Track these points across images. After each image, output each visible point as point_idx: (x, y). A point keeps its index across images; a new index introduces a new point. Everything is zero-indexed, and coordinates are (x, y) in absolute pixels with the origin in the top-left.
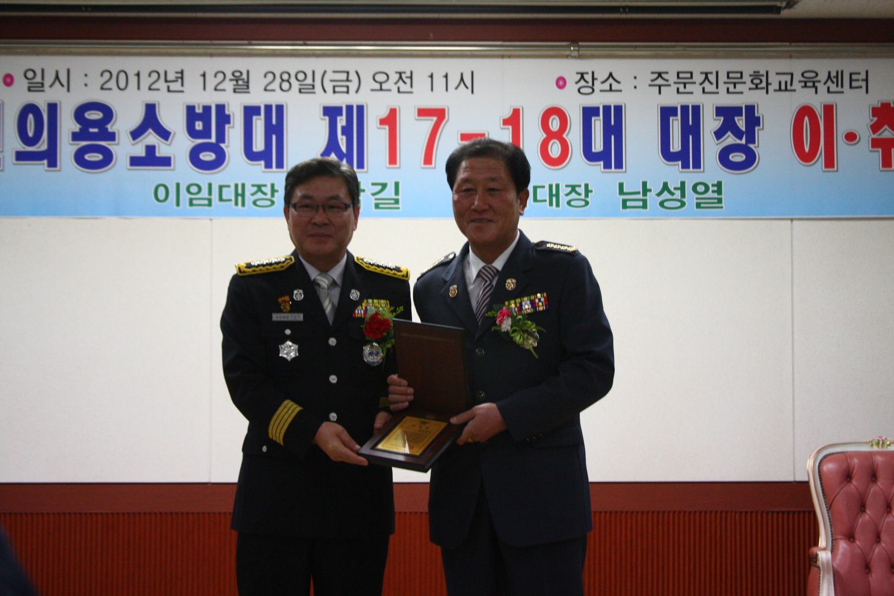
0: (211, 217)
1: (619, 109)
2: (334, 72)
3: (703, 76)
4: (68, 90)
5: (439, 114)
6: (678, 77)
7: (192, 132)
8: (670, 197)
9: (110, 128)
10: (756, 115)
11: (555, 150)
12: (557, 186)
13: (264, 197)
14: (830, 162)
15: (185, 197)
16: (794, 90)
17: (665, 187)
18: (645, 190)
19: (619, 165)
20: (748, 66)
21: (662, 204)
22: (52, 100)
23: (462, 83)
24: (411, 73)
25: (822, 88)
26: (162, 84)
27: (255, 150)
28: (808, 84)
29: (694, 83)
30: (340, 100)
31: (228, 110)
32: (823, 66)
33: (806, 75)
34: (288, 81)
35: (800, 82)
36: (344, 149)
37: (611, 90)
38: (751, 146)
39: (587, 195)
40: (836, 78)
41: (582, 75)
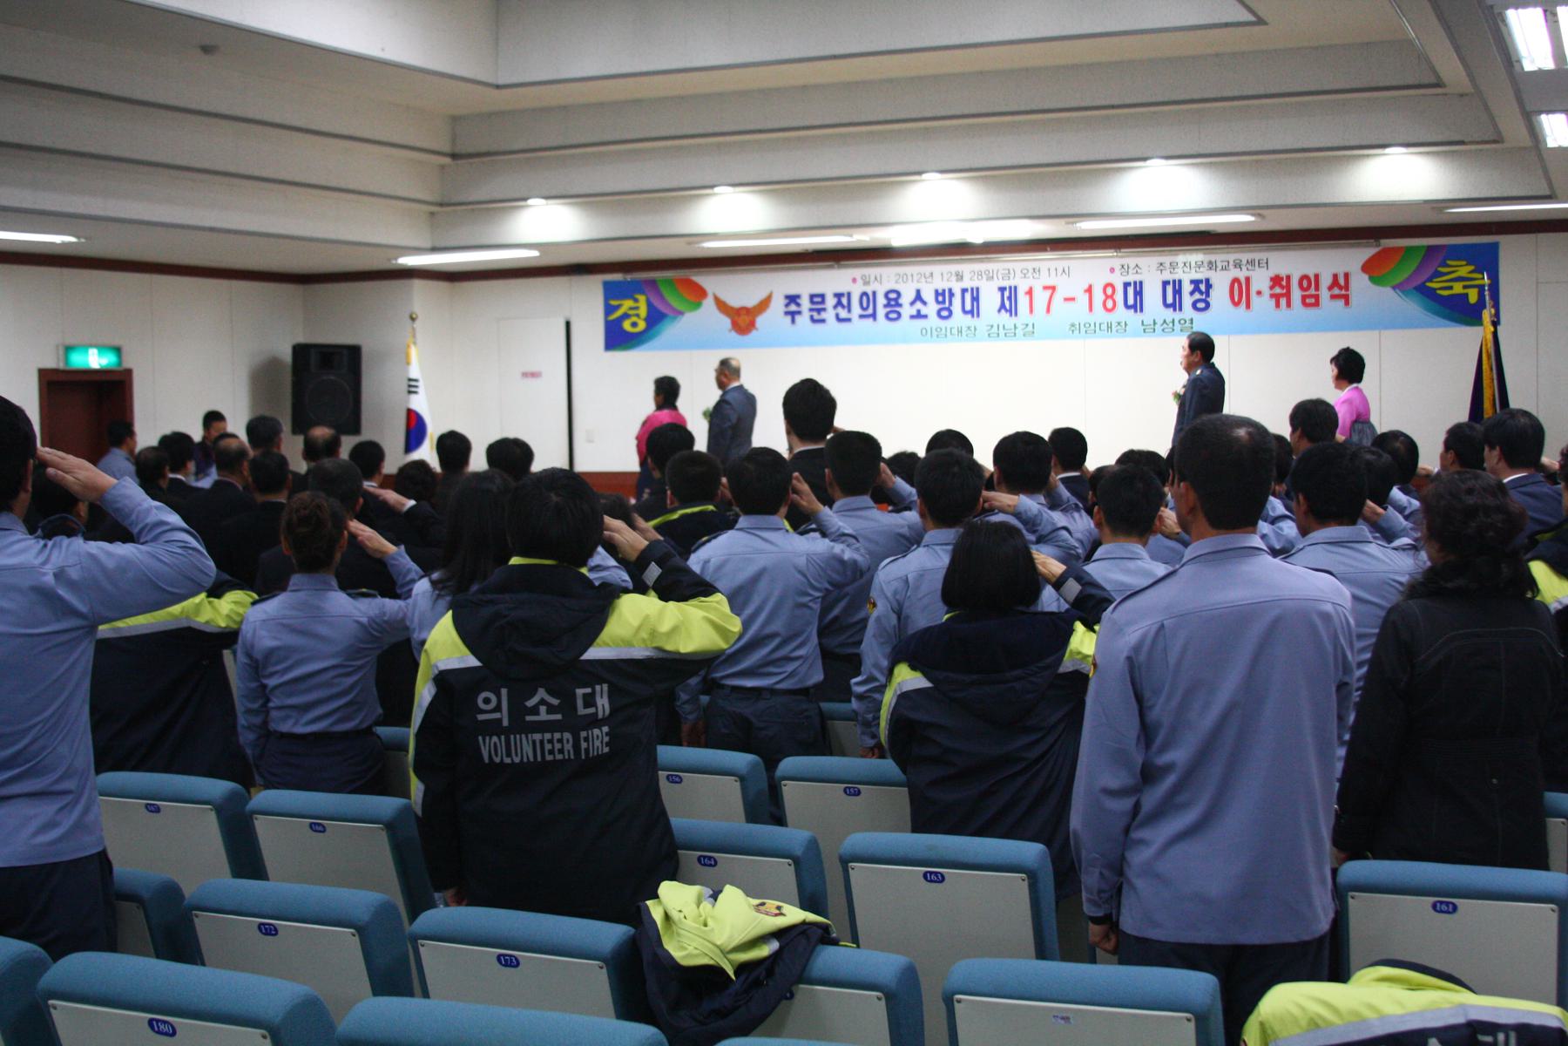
1: (1141, 283)
5: (1053, 288)
7: (937, 302)
11: (1110, 304)
14: (1248, 306)
15: (935, 333)
17: (1165, 321)
18: (1155, 323)
19: (1141, 310)
21: (1163, 330)
25: (1244, 268)
26: (923, 280)
30: (1006, 284)
32: (1245, 257)
36: (1008, 307)
38: (1208, 299)
40: (1251, 262)
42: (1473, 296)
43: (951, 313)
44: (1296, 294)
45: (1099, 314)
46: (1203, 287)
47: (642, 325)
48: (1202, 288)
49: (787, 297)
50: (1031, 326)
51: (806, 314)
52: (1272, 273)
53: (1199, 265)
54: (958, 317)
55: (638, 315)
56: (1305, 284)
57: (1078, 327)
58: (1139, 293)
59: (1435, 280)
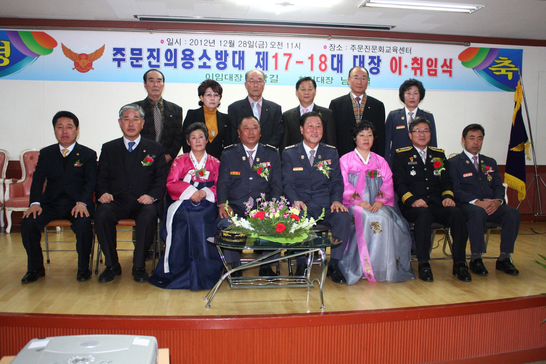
1: (341, 55)
9: (193, 57)
11: (323, 67)
12: (324, 77)
13: (238, 78)
14: (400, 73)
19: (341, 72)
20: (378, 44)
26: (208, 44)
28: (395, 51)
30: (261, 50)
32: (399, 45)
36: (262, 64)
38: (378, 68)
39: (332, 80)
42: (510, 76)
43: (225, 67)
44: (425, 68)
46: (376, 61)
47: (6, 62)
48: (376, 61)
49: (115, 49)
50: (275, 77)
51: (128, 61)
53: (374, 48)
55: (3, 55)
59: (492, 66)
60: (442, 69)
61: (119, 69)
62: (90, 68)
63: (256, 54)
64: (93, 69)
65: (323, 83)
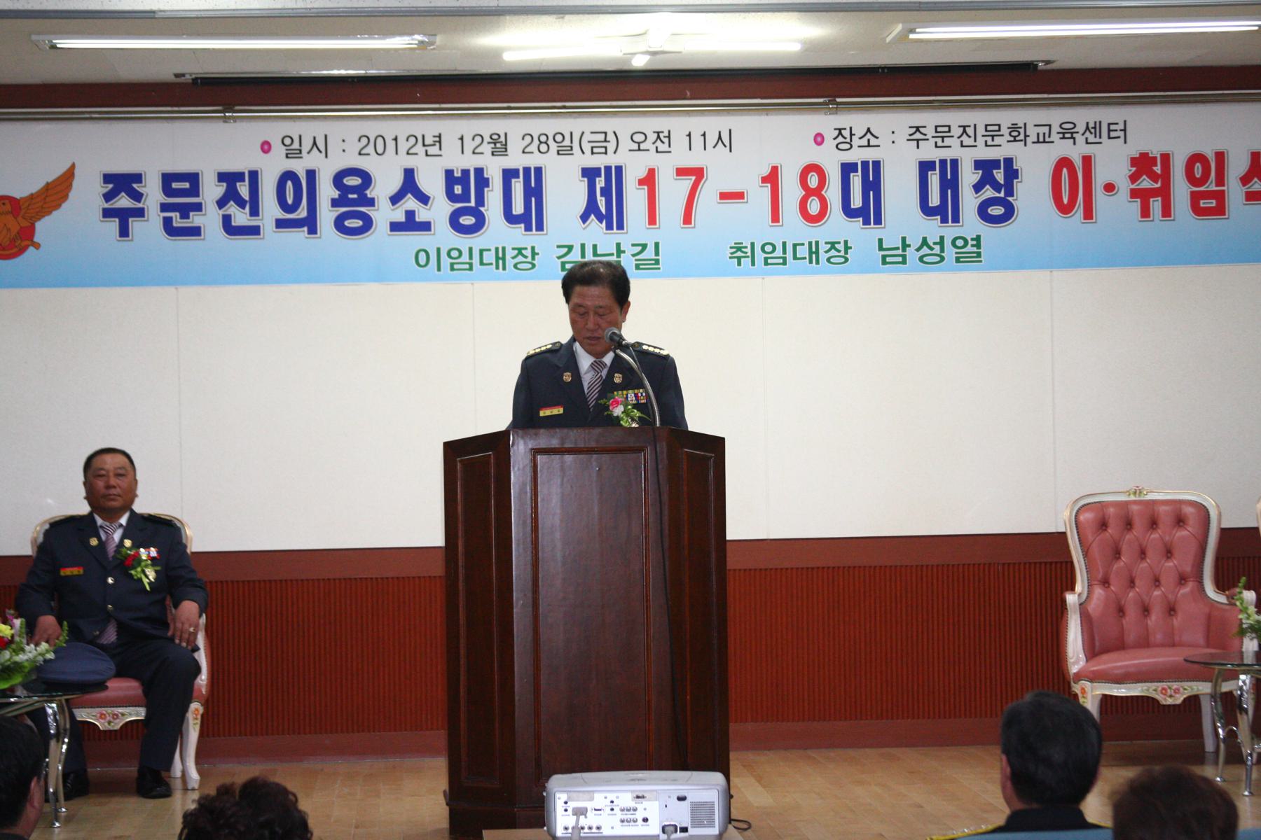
0: (473, 282)
1: (877, 164)
2: (592, 133)
3: (962, 129)
4: (326, 156)
5: (698, 174)
6: (936, 132)
7: (451, 196)
8: (929, 252)
10: (1015, 167)
11: (814, 207)
12: (817, 243)
14: (1088, 214)
15: (446, 261)
16: (1053, 142)
17: (925, 240)
18: (905, 245)
19: (878, 221)
20: (1006, 117)
21: (921, 259)
22: (311, 167)
23: (720, 141)
24: (669, 132)
26: (419, 149)
27: (514, 213)
28: (1067, 135)
29: (952, 137)
30: (598, 161)
31: (487, 174)
32: (1081, 116)
33: (1064, 126)
34: (546, 143)
35: (1058, 133)
36: (603, 211)
37: (869, 146)
39: (846, 252)
40: (1094, 129)
41: (840, 130)
43: (480, 223)
44: (1181, 190)
45: (794, 228)
46: (999, 176)
49: (108, 178)
50: (651, 248)
51: (155, 217)
52: (1134, 149)
53: (993, 132)
54: (497, 231)
56: (1198, 170)
57: (749, 250)
58: (873, 185)
60: (1245, 189)
61: (124, 245)
62: (28, 242)
63: (583, 176)
64: (37, 246)
65: (817, 263)
